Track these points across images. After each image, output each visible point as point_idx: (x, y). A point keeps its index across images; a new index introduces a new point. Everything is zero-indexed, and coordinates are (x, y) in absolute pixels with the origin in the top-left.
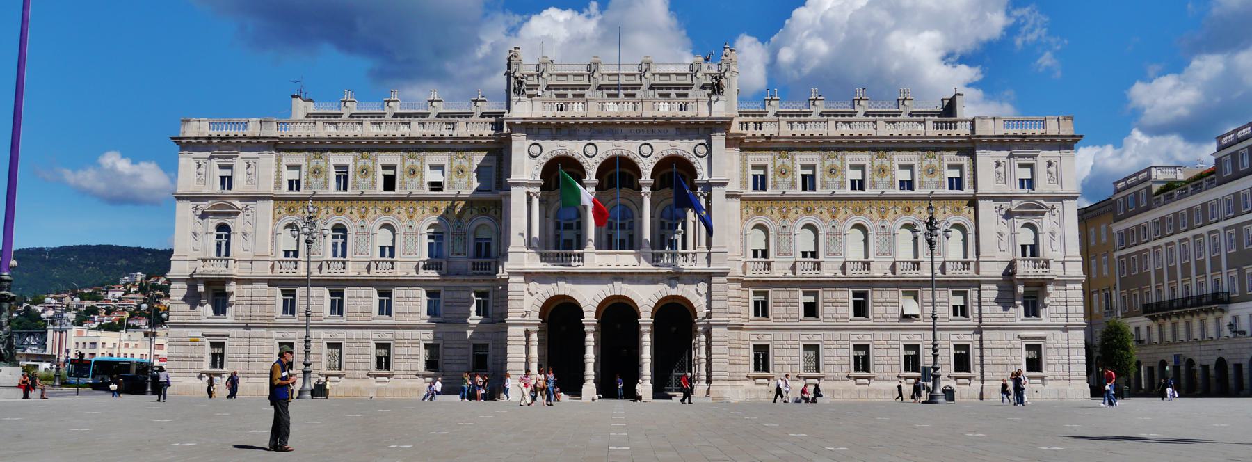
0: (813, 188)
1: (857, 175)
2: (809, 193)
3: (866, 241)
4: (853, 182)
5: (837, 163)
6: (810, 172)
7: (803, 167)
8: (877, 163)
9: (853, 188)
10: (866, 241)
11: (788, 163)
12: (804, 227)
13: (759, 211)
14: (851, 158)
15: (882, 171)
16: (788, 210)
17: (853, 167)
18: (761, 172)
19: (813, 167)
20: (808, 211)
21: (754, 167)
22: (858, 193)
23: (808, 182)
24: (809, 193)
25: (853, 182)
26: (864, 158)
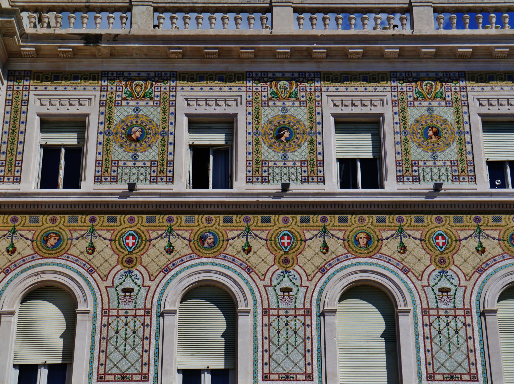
0: (226, 180)
1: (360, 146)
2: (212, 194)
3: (392, 337)
4: (347, 166)
5: (298, 112)
6: (218, 139)
7: (196, 124)
8: (414, 113)
9: (347, 180)
10: (392, 337)
11: (151, 112)
12: (189, 295)
13: (50, 245)
14: (335, 99)
15: (433, 133)
16: (143, 241)
17: (345, 125)
18: (70, 139)
19: (226, 124)
20: (206, 245)
21: (48, 124)
22: (360, 194)
23: (211, 165)
24: (212, 194)
25: (347, 166)
26: (378, 99)
